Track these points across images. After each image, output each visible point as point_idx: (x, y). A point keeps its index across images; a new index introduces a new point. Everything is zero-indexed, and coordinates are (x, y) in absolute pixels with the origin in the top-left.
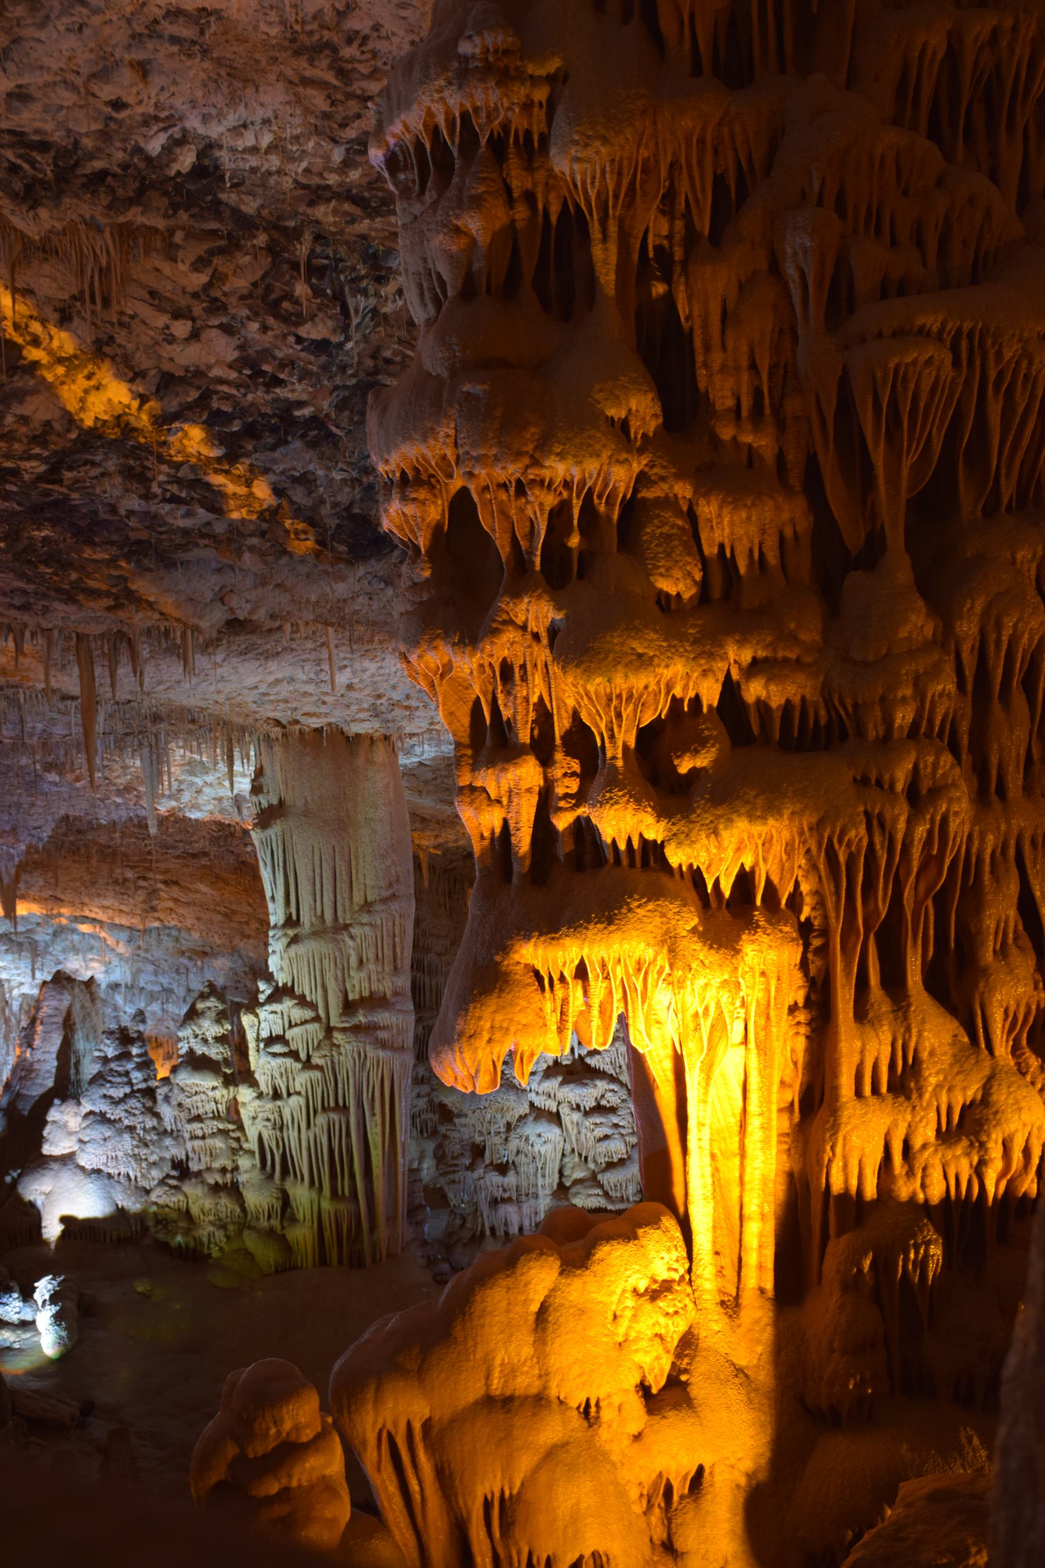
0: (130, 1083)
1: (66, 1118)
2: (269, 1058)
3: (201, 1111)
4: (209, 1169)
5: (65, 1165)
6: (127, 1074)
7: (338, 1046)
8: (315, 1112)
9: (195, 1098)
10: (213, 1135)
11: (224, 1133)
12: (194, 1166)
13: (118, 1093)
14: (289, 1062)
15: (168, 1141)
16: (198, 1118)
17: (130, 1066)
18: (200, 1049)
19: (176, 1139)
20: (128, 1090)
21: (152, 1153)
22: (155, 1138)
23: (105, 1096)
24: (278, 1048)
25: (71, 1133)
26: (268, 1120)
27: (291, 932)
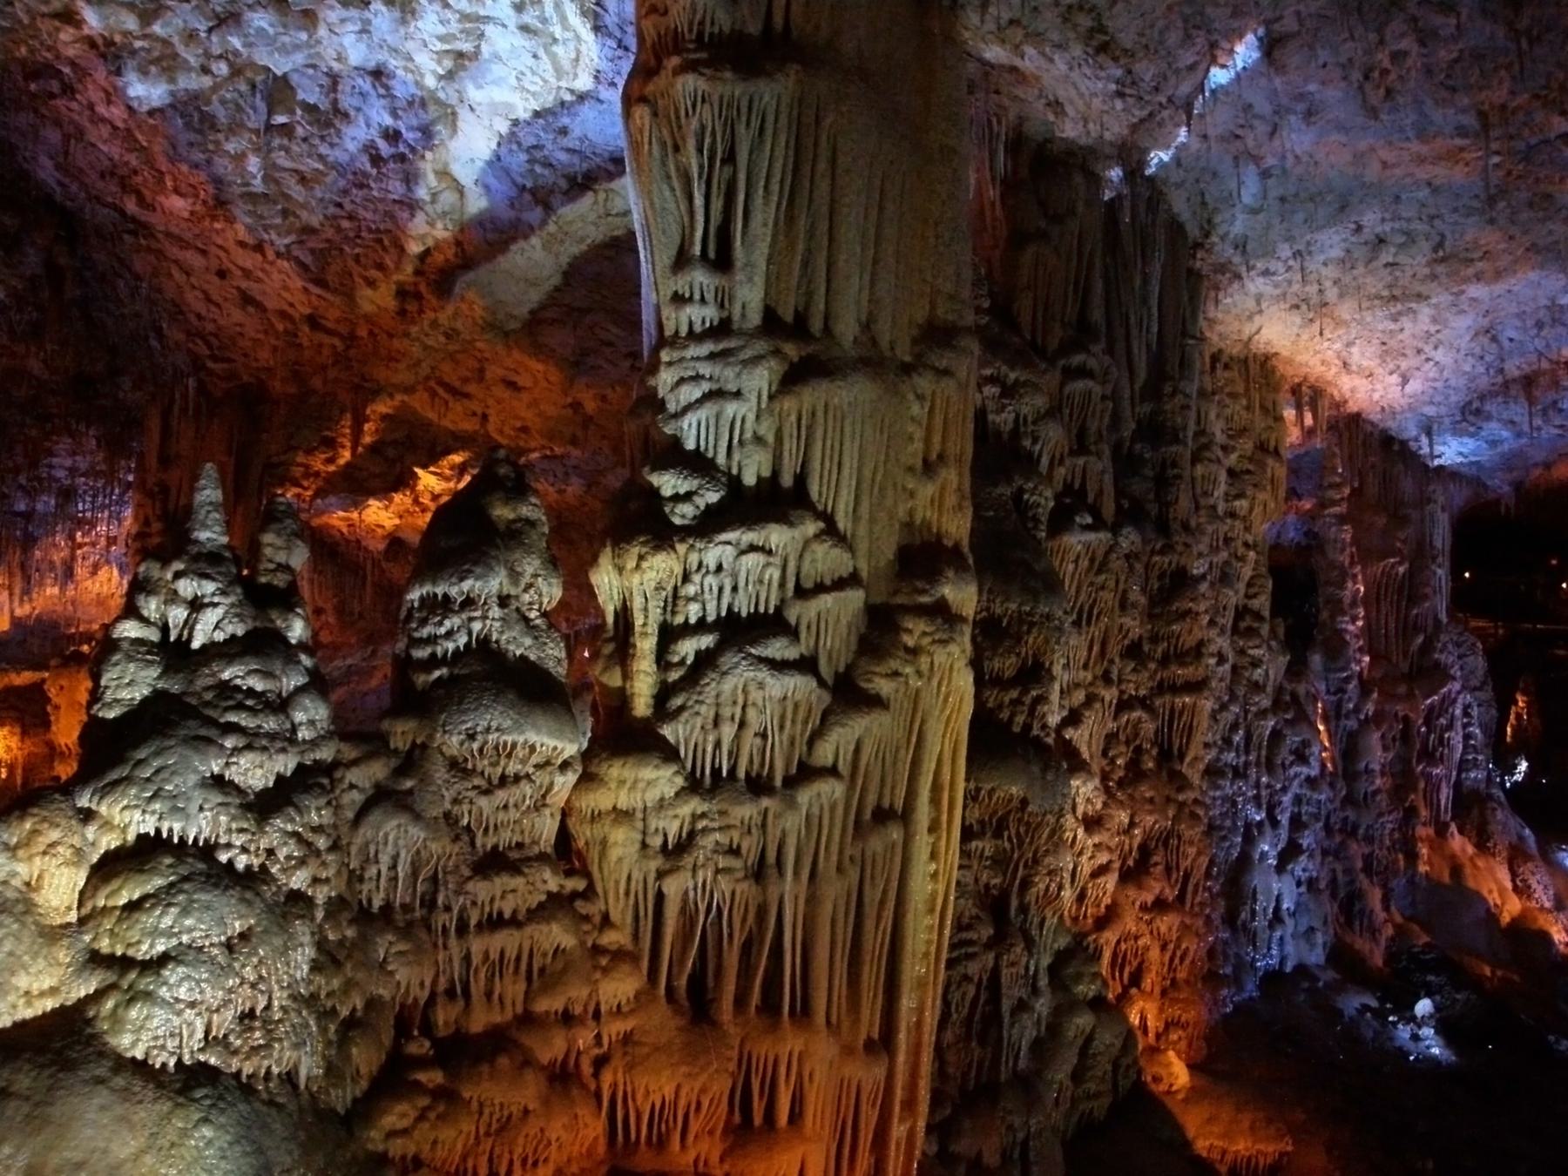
0: (288, 739)
1: (22, 869)
2: (764, 674)
3: (506, 837)
4: (527, 1019)
5: (69, 1066)
6: (281, 705)
7: (914, 652)
8: (857, 822)
9: (501, 796)
10: (540, 913)
11: (557, 904)
12: (578, 1010)
13: (254, 772)
14: (797, 685)
15: (385, 945)
16: (495, 863)
17: (293, 681)
18: (518, 644)
19: (406, 932)
20: (285, 764)
21: (349, 986)
22: (350, 933)
23: (218, 782)
24: (777, 648)
25: (53, 935)
26: (734, 851)
27: (792, 350)
